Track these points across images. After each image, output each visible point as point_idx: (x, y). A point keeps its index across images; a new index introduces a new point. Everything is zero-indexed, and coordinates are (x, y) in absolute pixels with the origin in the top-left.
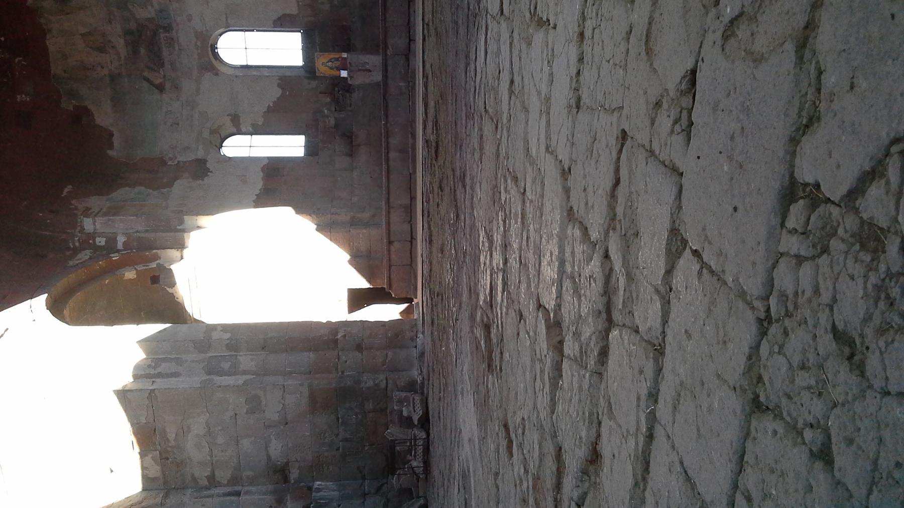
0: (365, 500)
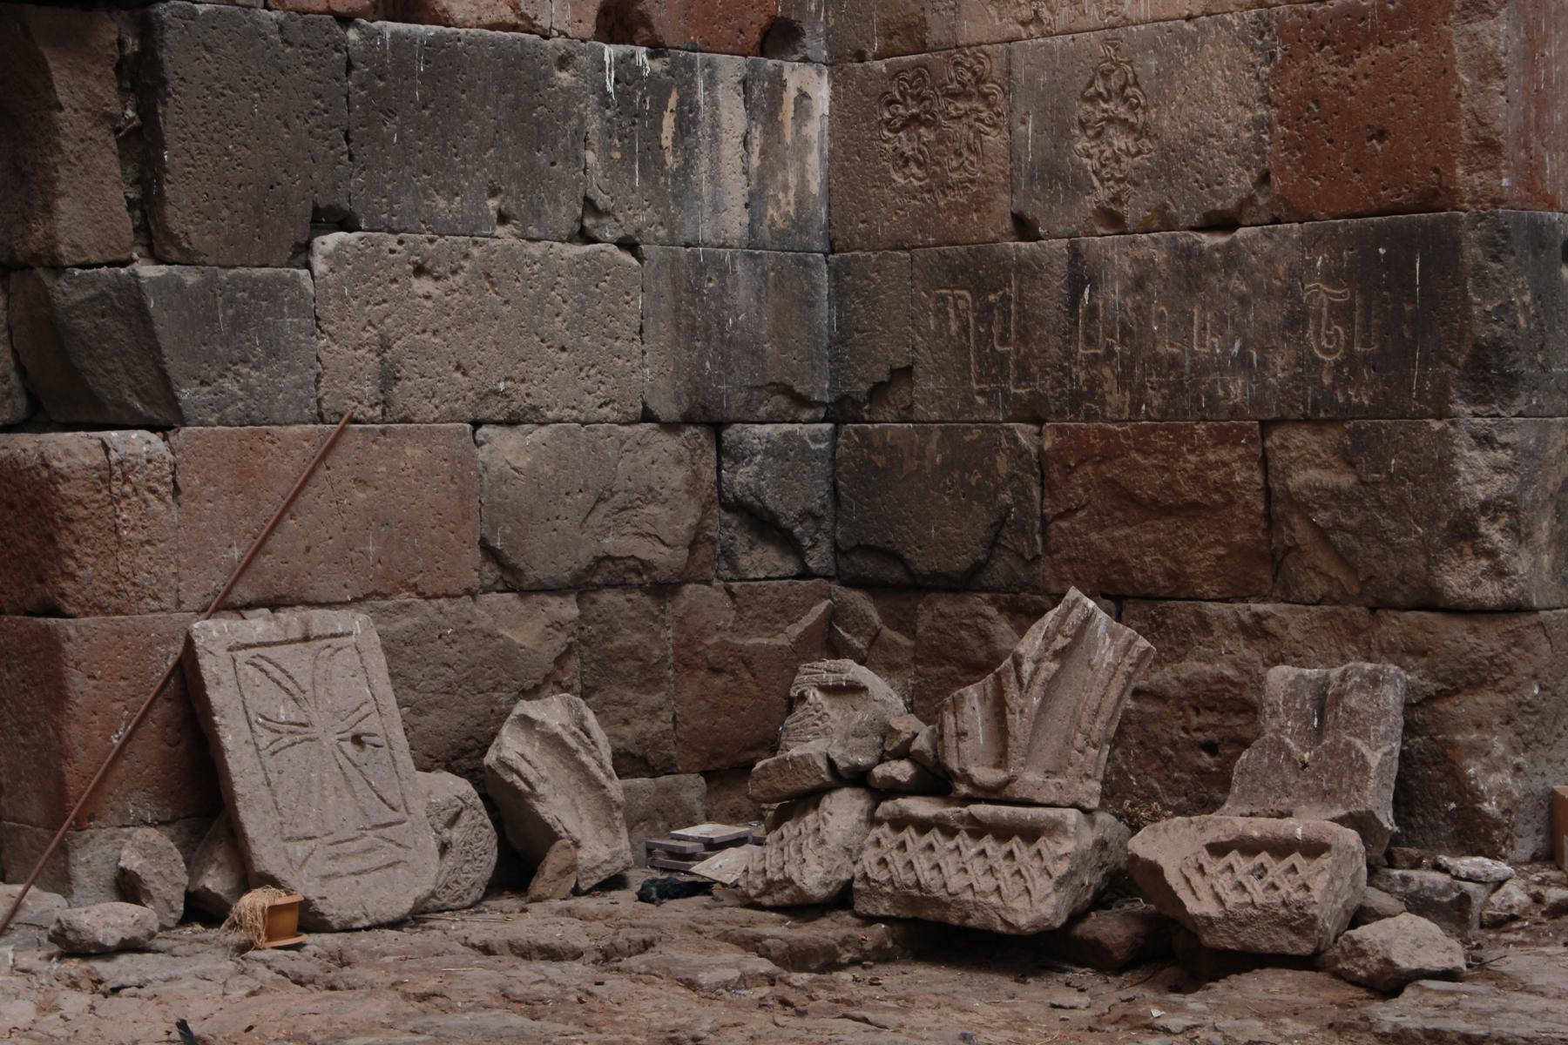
0: (671, 427)
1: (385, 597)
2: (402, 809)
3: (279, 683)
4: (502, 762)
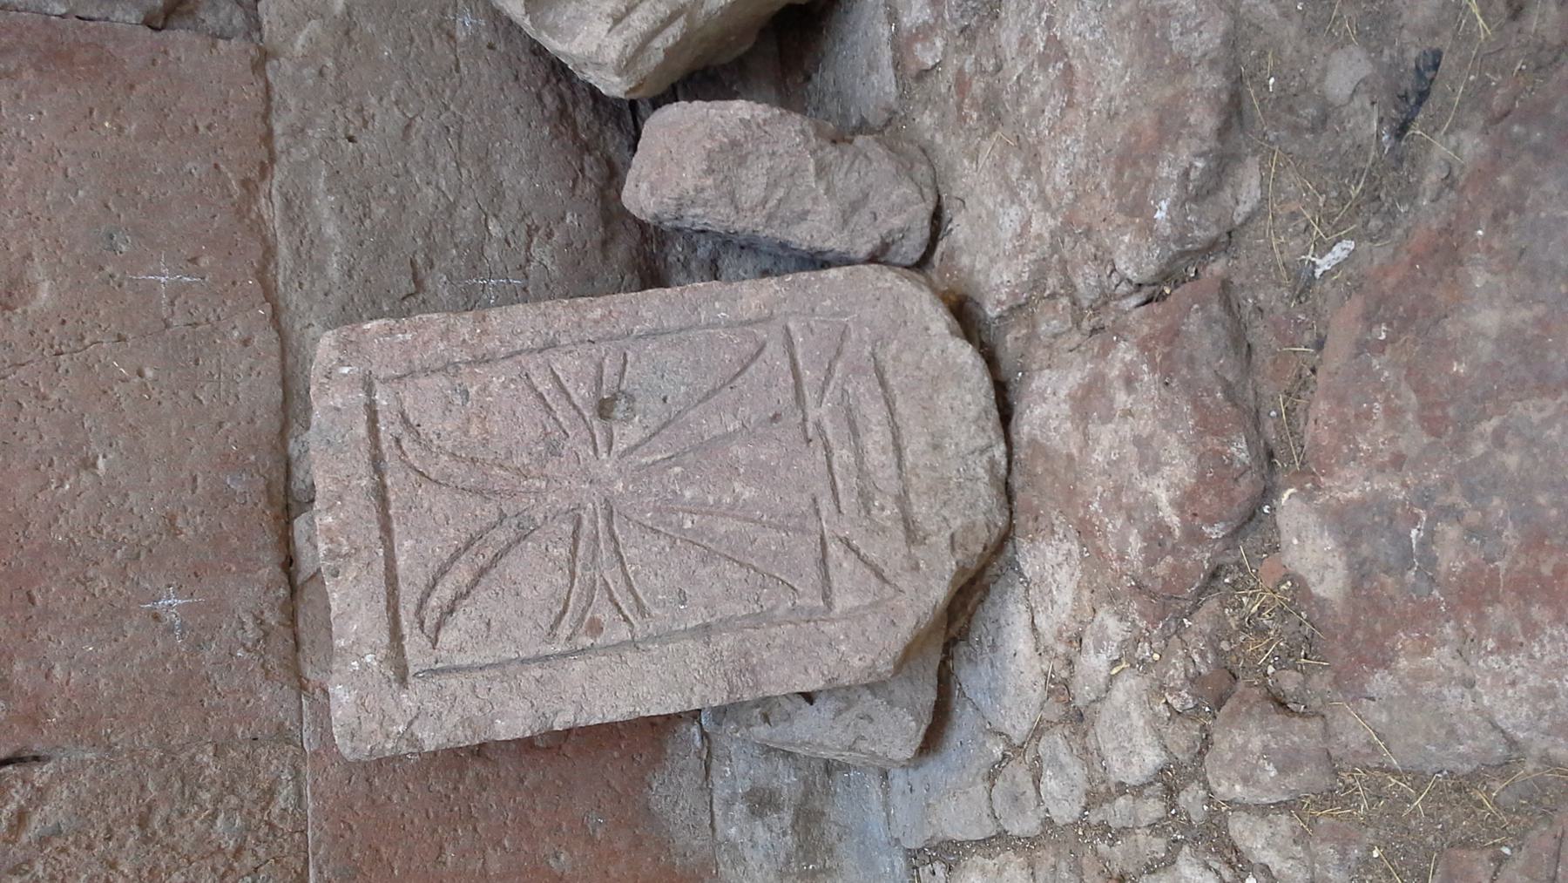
1: (269, 252)
2: (761, 333)
3: (483, 571)
4: (625, 66)
